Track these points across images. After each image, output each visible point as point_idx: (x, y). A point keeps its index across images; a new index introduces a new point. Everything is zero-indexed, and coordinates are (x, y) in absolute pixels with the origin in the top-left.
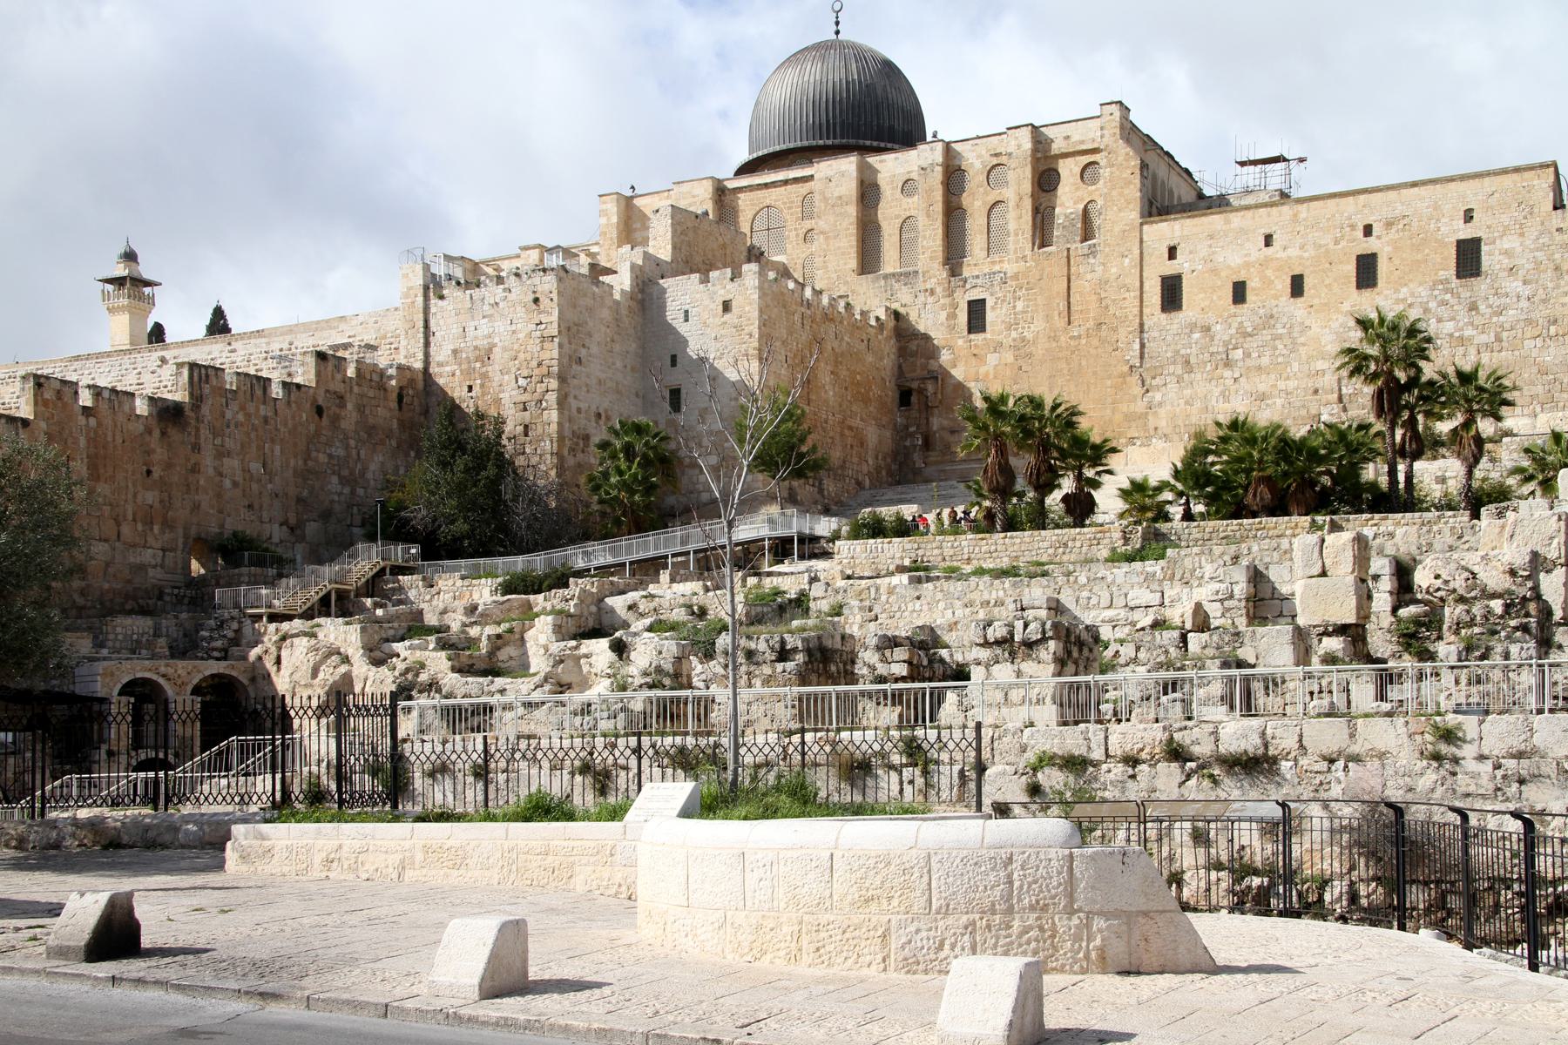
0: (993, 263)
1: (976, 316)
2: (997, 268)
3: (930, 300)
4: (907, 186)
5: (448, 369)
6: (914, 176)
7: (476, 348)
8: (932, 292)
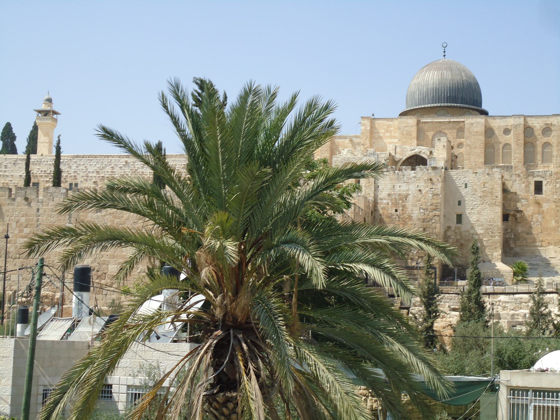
0: (545, 167)
1: (538, 187)
2: (546, 169)
3: (518, 178)
4: (507, 131)
5: (385, 201)
6: (509, 127)
7: (400, 194)
8: (519, 175)
